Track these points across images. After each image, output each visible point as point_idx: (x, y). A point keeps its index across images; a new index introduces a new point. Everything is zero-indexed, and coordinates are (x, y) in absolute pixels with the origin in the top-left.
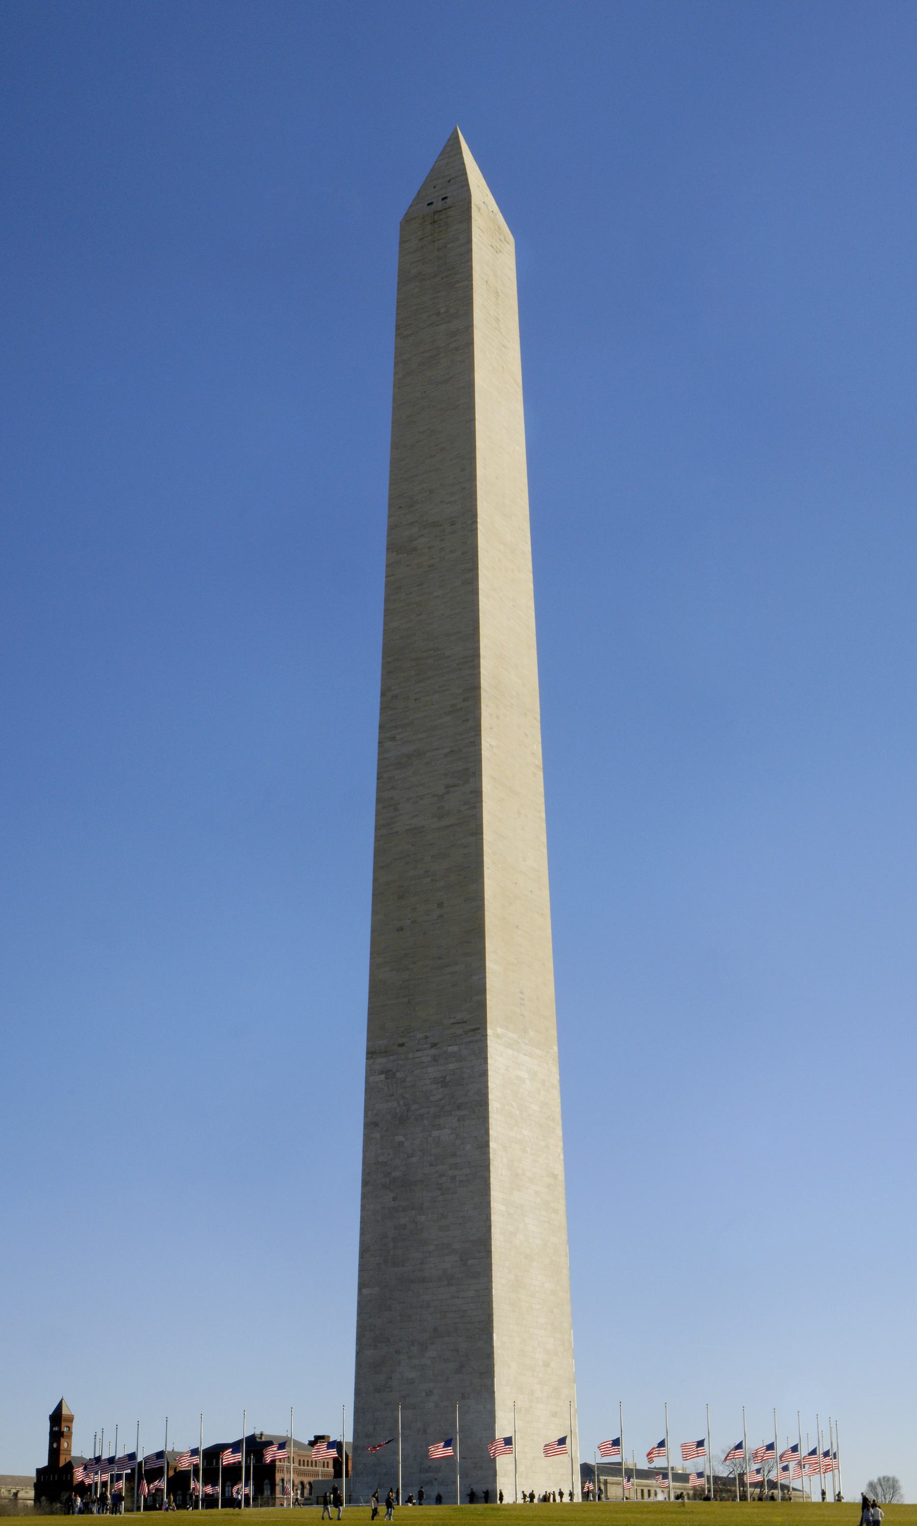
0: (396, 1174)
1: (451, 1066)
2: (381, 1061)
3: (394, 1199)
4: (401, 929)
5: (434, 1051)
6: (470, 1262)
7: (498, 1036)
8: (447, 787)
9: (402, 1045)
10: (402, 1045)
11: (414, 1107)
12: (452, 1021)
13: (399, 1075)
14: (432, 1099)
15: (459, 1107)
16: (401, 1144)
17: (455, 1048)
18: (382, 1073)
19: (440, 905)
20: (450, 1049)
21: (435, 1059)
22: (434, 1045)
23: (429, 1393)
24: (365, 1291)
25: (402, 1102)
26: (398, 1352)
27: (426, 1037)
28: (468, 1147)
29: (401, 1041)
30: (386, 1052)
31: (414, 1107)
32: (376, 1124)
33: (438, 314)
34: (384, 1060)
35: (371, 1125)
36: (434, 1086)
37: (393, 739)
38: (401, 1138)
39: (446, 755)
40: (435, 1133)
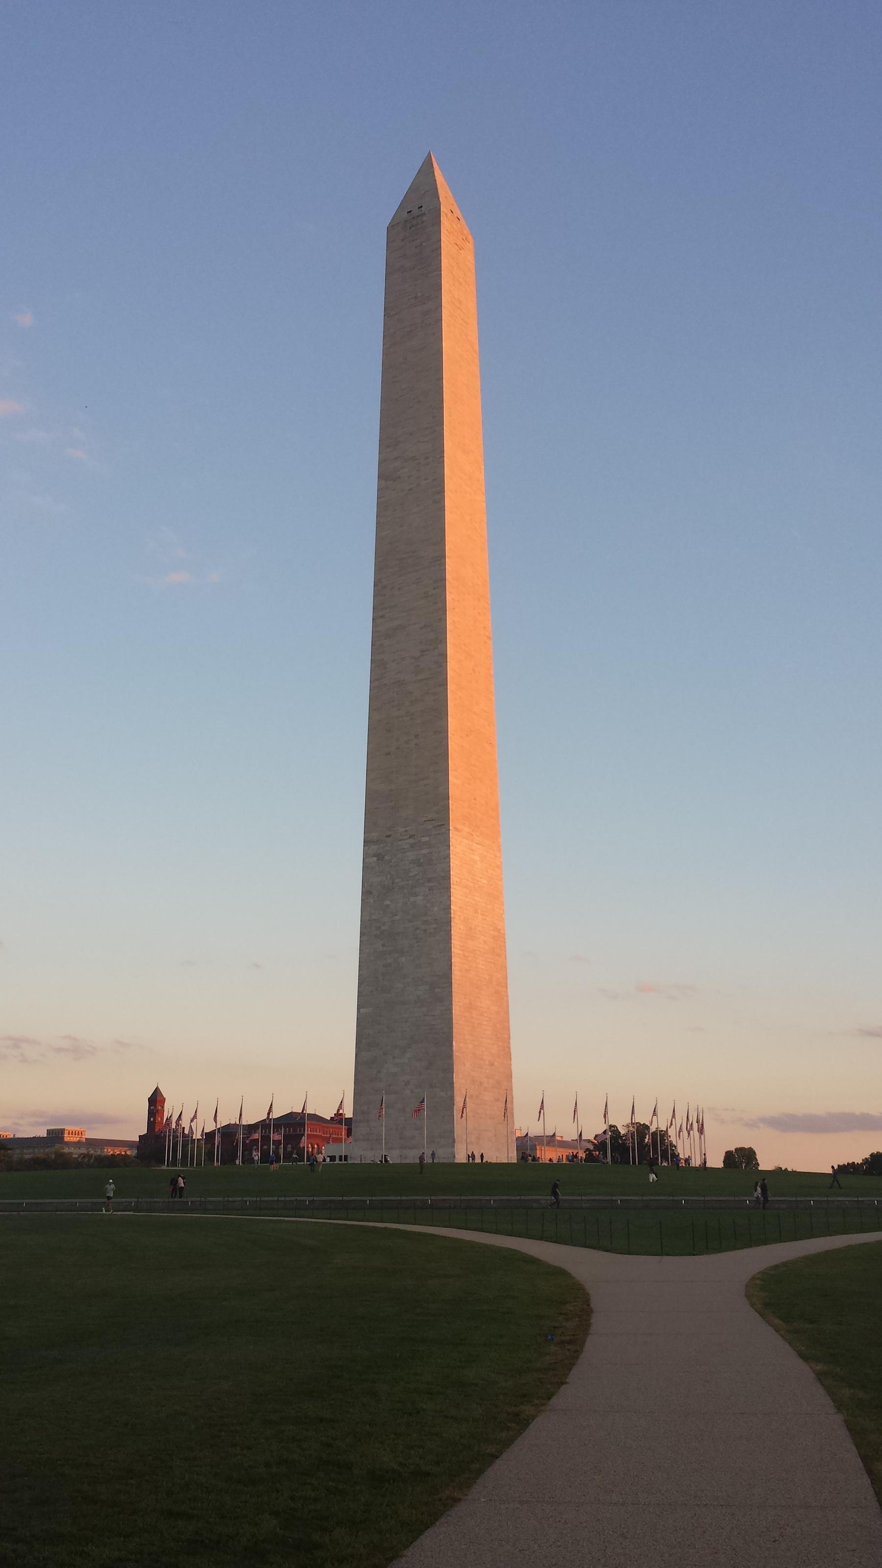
1: (424, 852)
2: (374, 848)
3: (383, 945)
4: (389, 754)
5: (411, 841)
7: (456, 829)
9: (389, 836)
10: (389, 836)
12: (424, 819)
13: (387, 858)
14: (411, 874)
15: (429, 880)
16: (388, 906)
17: (427, 839)
18: (374, 856)
19: (416, 736)
20: (424, 839)
21: (412, 846)
24: (362, 1010)
25: (389, 877)
26: (385, 1054)
27: (406, 831)
28: (436, 909)
30: (377, 842)
31: (396, 881)
32: (370, 893)
33: (416, 297)
35: (366, 893)
37: (383, 617)
38: (388, 902)
39: (421, 628)
40: (412, 899)
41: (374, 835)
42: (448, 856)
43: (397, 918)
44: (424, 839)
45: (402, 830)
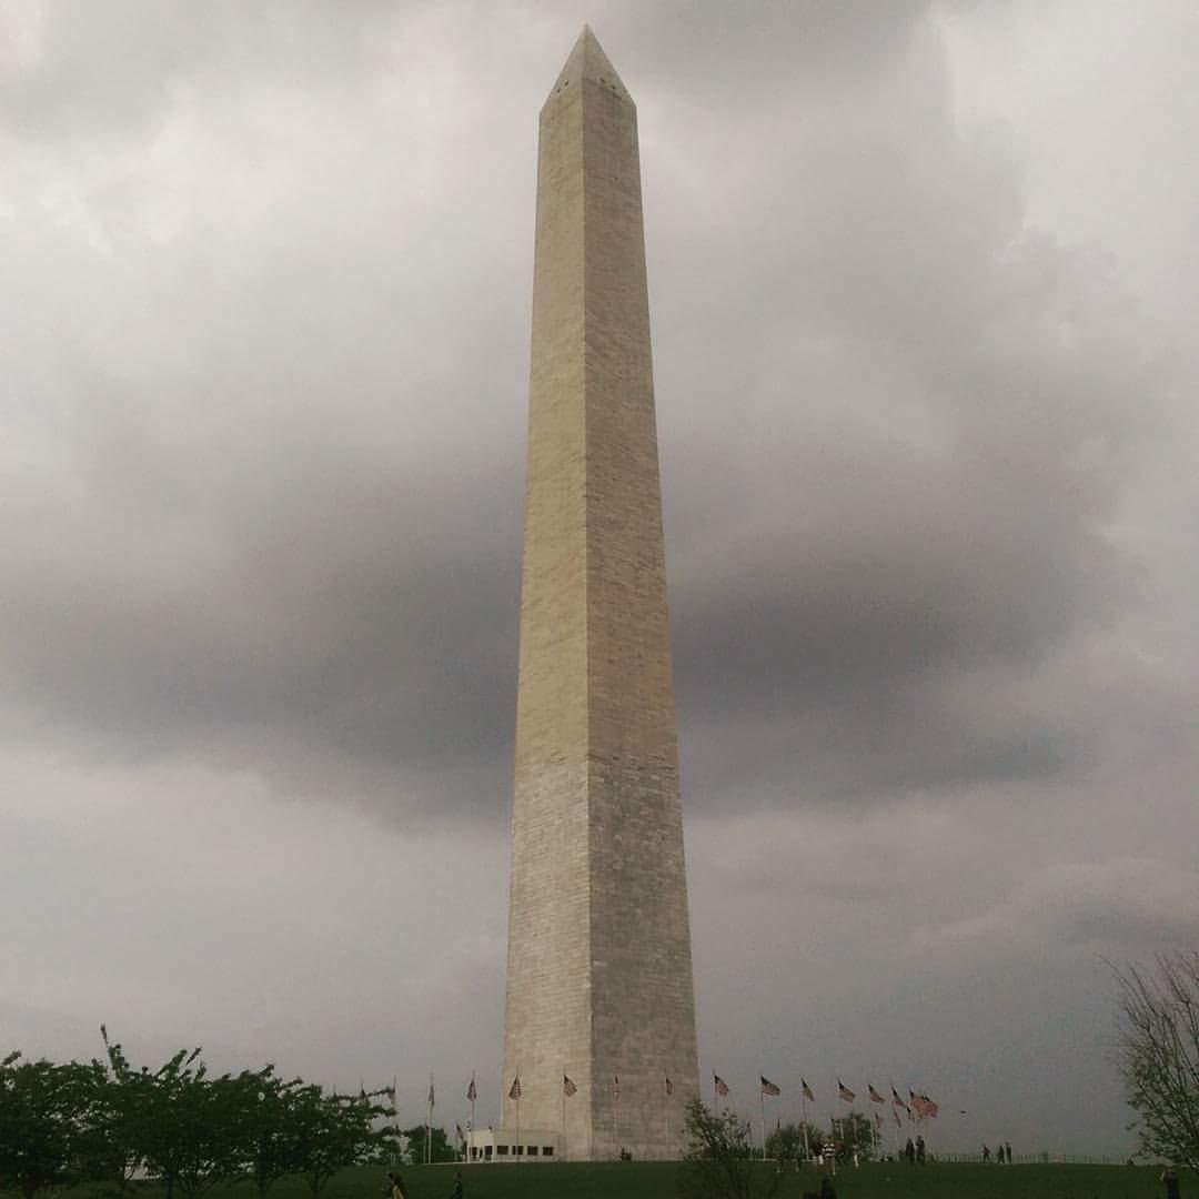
3: (616, 887)
6: (676, 957)
8: (640, 562)
9: (615, 758)
11: (628, 815)
13: (616, 784)
15: (663, 826)
18: (602, 777)
20: (654, 777)
22: (640, 769)
28: (671, 862)
29: (617, 755)
34: (603, 767)
36: (641, 804)
37: (597, 499)
38: (618, 837)
39: (638, 537)
40: (646, 842)
41: (600, 751)
44: (654, 777)
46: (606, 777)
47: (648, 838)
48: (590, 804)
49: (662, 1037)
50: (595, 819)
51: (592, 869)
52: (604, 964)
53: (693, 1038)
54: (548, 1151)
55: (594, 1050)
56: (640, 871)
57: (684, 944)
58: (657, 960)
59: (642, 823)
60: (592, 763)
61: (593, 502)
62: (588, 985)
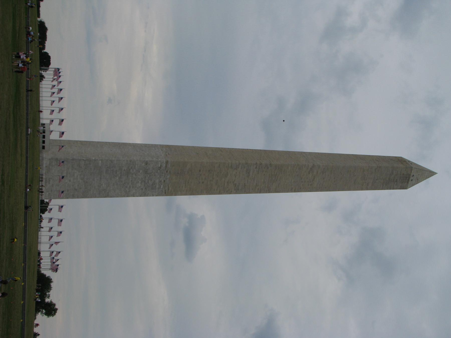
0: (131, 171)
2: (164, 165)
3: (124, 170)
4: (200, 171)
5: (163, 181)
13: (159, 171)
15: (146, 189)
16: (139, 172)
17: (162, 187)
18: (161, 166)
19: (203, 182)
21: (160, 181)
22: (164, 181)
23: (70, 181)
28: (134, 191)
29: (168, 171)
30: (166, 167)
37: (256, 168)
38: (141, 172)
39: (245, 184)
40: (140, 182)
42: (153, 196)
43: (134, 175)
45: (168, 177)
46: (160, 167)
47: (141, 183)
48: (151, 161)
49: (78, 186)
50: (147, 163)
51: (131, 161)
52: (100, 165)
53: (78, 198)
54: (44, 147)
55: (73, 159)
56: (130, 179)
57: (107, 195)
58: (102, 185)
59: (146, 181)
60: (165, 162)
61: (255, 166)
62: (93, 158)
